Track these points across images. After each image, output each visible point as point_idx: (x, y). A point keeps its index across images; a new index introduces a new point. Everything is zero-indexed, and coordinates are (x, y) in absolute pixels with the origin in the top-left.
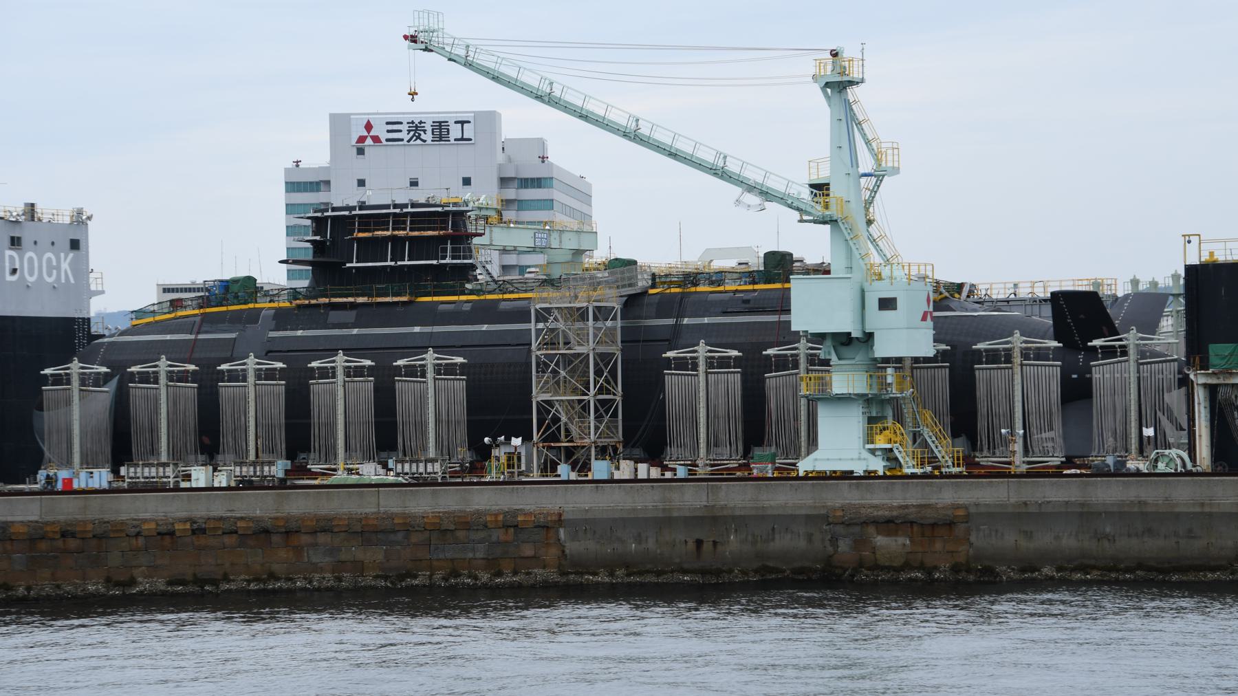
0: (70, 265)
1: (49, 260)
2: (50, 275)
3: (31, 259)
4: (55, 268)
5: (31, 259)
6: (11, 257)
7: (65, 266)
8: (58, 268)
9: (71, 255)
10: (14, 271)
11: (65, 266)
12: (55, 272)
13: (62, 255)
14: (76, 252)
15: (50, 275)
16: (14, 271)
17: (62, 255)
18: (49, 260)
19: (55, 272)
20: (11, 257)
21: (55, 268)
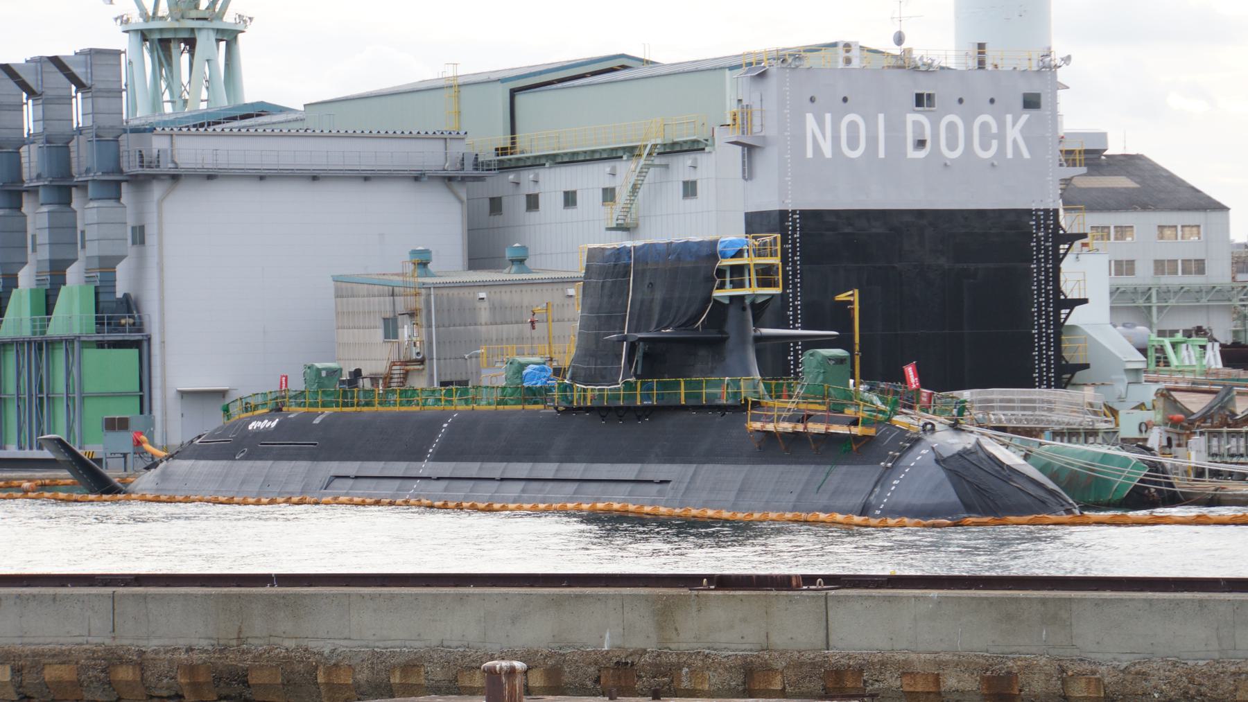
0: (1021, 131)
1: (984, 126)
2: (985, 146)
3: (952, 127)
4: (994, 137)
5: (952, 127)
6: (917, 124)
7: (1013, 133)
8: (1001, 137)
9: (1025, 117)
10: (921, 144)
11: (1013, 133)
12: (995, 143)
13: (1009, 118)
14: (1034, 112)
15: (985, 146)
16: (921, 144)
17: (1009, 118)
18: (984, 126)
19: (995, 143)
20: (917, 124)
21: (994, 137)
